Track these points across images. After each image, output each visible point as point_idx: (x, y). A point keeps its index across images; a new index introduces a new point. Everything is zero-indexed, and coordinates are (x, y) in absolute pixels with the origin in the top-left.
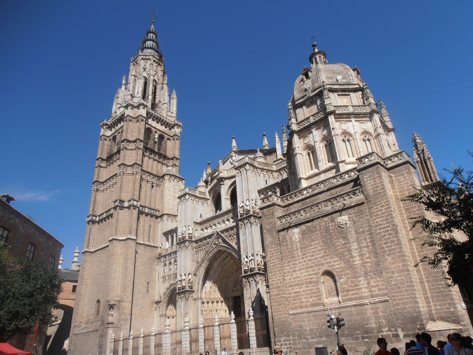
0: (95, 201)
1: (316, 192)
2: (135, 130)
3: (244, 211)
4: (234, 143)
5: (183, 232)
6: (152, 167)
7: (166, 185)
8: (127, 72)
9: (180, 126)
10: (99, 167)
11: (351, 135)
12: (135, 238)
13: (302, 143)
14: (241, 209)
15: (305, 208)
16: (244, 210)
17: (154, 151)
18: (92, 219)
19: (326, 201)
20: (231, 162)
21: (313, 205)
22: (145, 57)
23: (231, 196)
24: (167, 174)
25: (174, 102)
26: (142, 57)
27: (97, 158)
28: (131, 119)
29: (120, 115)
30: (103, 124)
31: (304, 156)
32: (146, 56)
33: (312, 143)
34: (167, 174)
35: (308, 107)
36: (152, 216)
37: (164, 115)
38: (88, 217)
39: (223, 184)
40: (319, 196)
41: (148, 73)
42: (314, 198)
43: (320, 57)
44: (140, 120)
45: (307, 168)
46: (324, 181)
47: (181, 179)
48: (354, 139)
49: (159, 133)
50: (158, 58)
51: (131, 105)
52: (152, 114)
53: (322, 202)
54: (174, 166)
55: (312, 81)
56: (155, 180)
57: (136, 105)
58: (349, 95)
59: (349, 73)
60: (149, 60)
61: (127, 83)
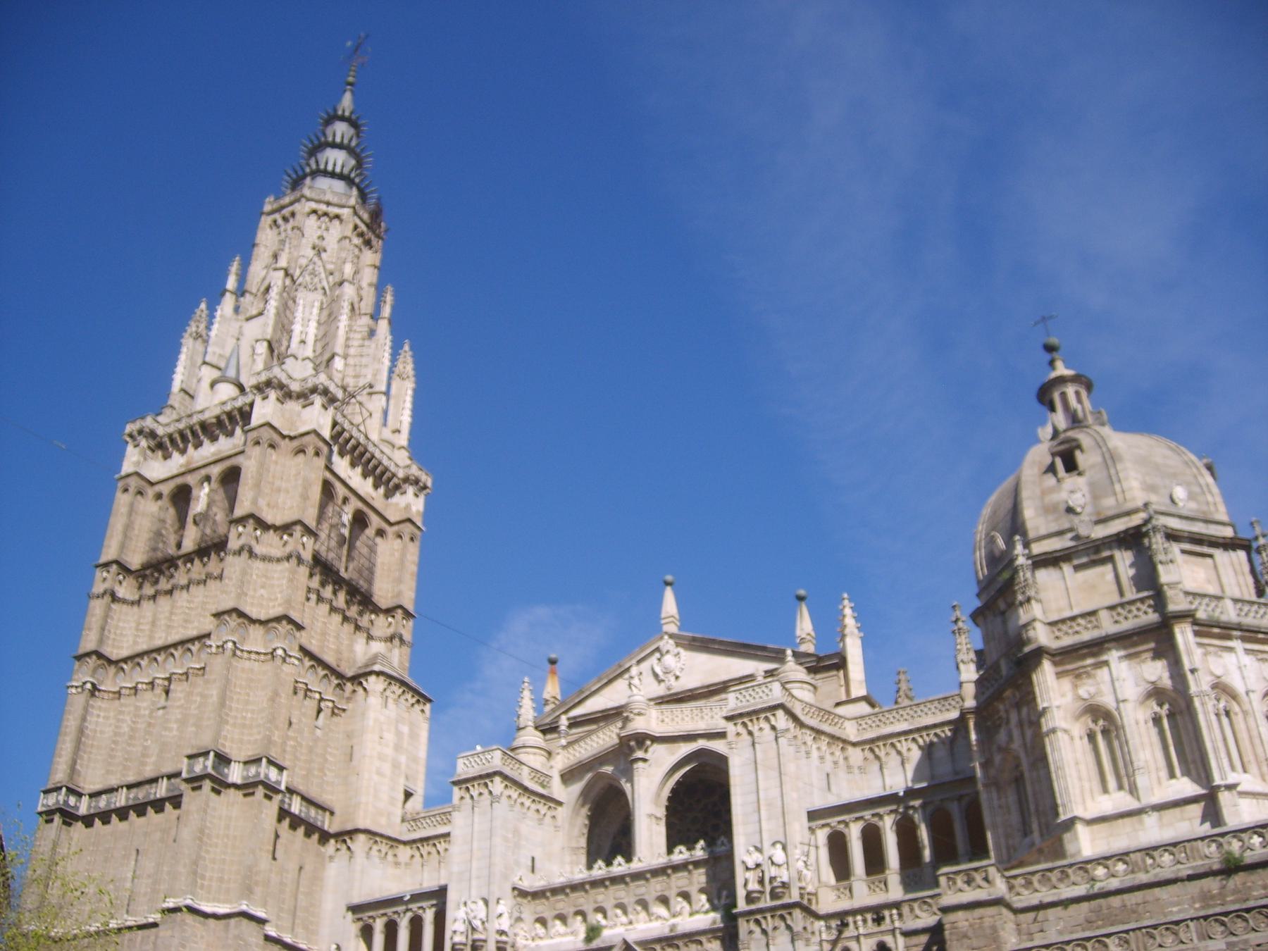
0: (81, 731)
1: (1143, 878)
2: (284, 485)
3: (761, 882)
4: (670, 605)
5: (477, 923)
6: (324, 634)
7: (372, 715)
8: (246, 249)
9: (425, 487)
10: (107, 598)
11: (1234, 696)
12: (260, 913)
13: (1069, 697)
14: (750, 875)
15: (1127, 932)
16: (761, 882)
17: (337, 573)
18: (66, 802)
19: (1206, 918)
20: (656, 675)
21: (1155, 927)
22: (323, 208)
23: (667, 808)
24: (378, 674)
25: (405, 391)
26: (314, 205)
27: (103, 559)
28: (275, 437)
29: (217, 411)
30: (140, 432)
31: (1077, 741)
32: (328, 204)
33: (1108, 701)
34: (378, 674)
35: (1077, 568)
36: (311, 829)
37: (374, 437)
38: (46, 792)
39: (645, 760)
40: (1157, 891)
41: (330, 267)
42: (1137, 897)
43: (1077, 394)
44: (310, 451)
45: (1087, 785)
46: (1175, 845)
47: (423, 698)
48: (1245, 713)
49: (354, 504)
50: (366, 216)
51: (281, 386)
52: (344, 430)
53: (1192, 919)
54: (396, 642)
55: (1092, 485)
56: (327, 689)
57: (295, 387)
58: (1211, 556)
59: (1202, 481)
60: (336, 222)
61: (241, 292)
